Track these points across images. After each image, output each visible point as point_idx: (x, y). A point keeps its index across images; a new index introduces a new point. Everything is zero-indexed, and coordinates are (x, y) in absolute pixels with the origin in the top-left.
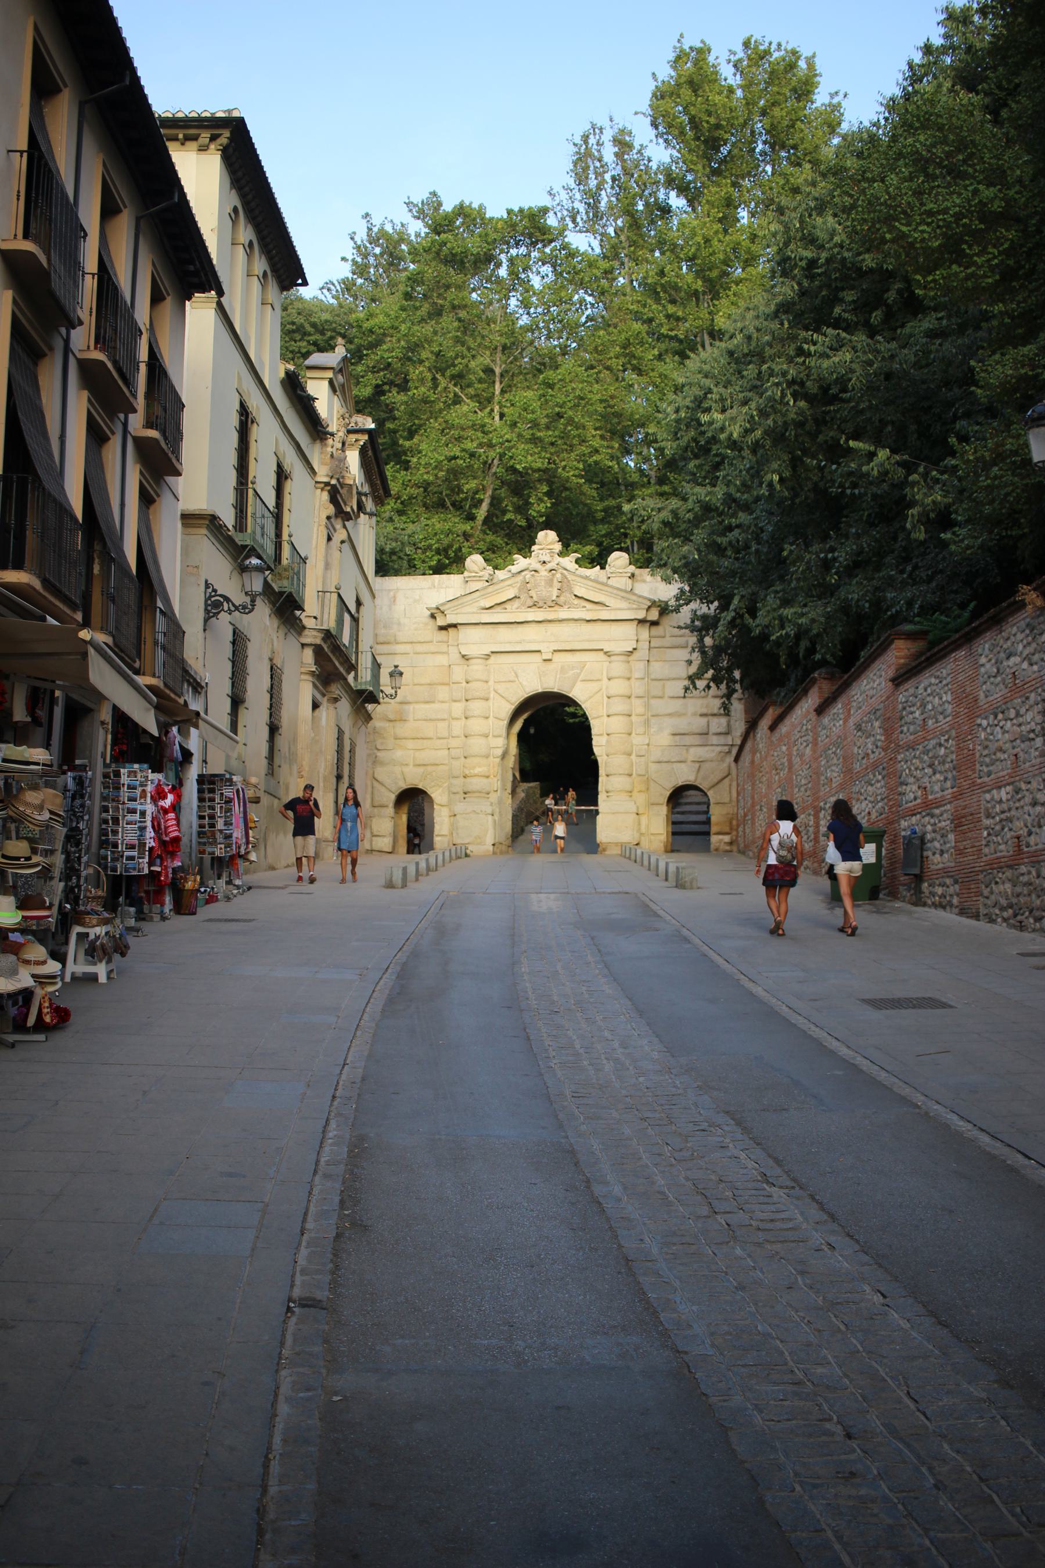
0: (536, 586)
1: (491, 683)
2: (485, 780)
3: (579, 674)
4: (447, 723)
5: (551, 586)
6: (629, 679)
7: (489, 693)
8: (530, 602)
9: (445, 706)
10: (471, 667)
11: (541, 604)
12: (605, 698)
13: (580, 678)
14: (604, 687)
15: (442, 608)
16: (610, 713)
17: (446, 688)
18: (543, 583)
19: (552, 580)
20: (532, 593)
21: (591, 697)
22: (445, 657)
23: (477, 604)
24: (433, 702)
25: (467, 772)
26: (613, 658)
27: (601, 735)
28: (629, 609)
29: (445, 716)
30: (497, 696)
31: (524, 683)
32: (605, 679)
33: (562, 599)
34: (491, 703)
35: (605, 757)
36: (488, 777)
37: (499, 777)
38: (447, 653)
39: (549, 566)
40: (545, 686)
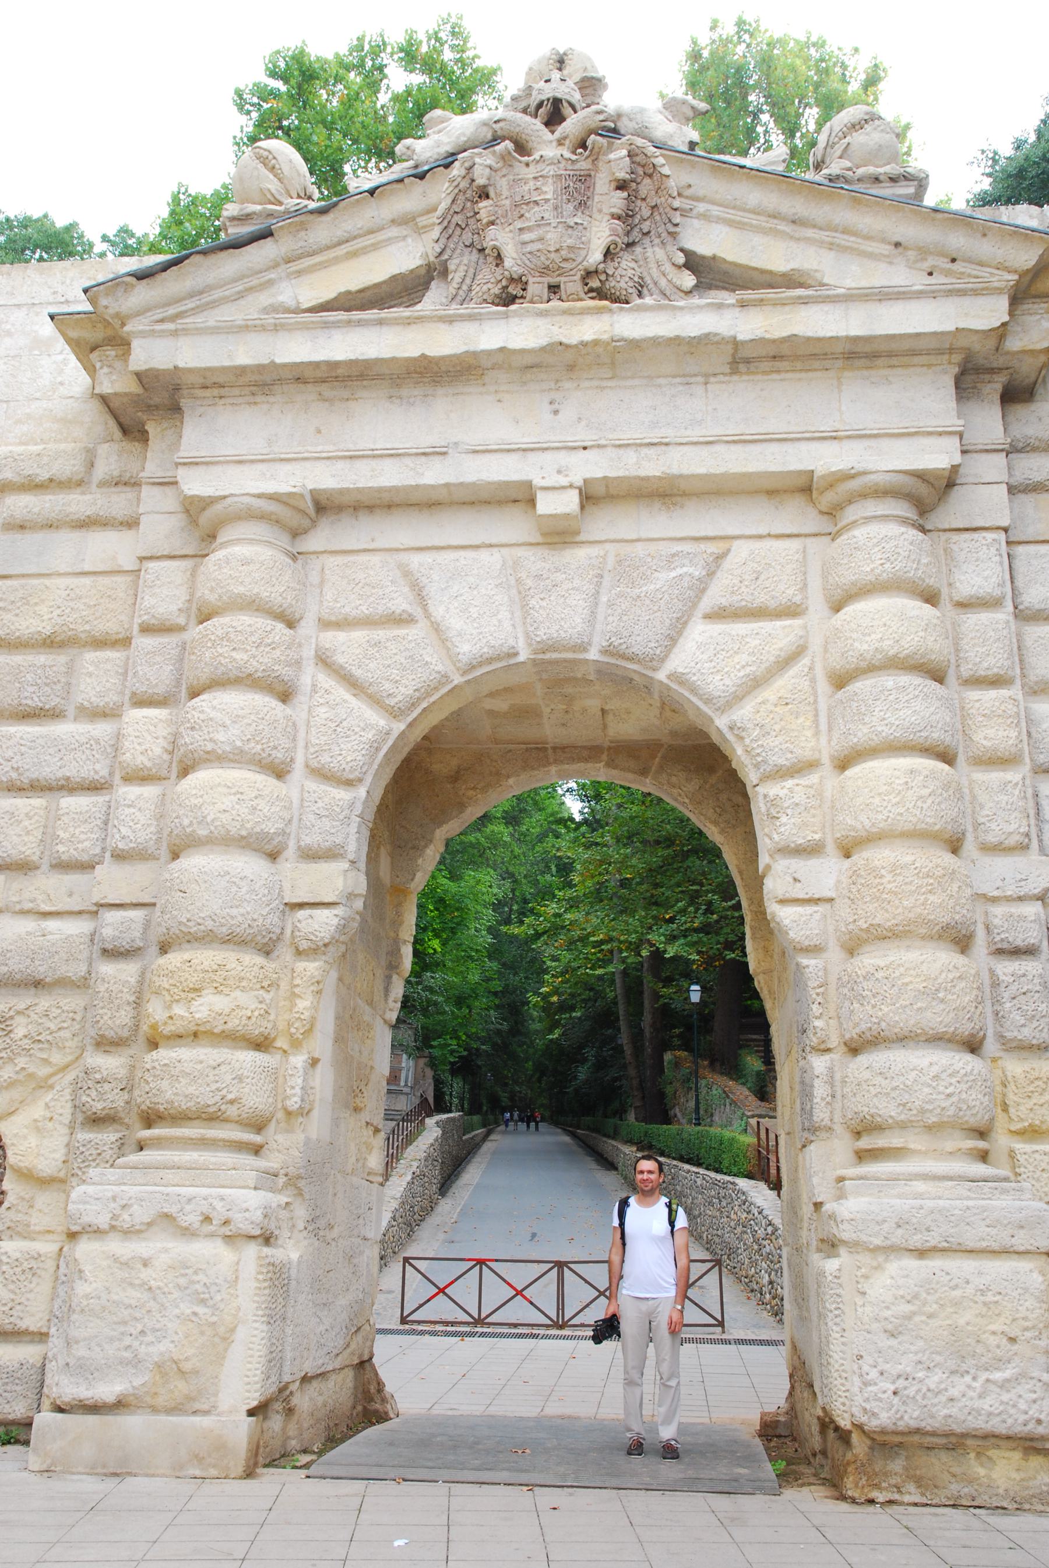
0: (522, 204)
1: (307, 628)
2: (247, 1057)
3: (701, 588)
4: (100, 799)
5: (582, 205)
6: (931, 598)
7: (298, 663)
8: (489, 281)
9: (102, 729)
10: (220, 554)
11: (536, 287)
12: (823, 686)
13: (707, 603)
14: (816, 644)
15: (111, 305)
16: (862, 734)
17: (113, 655)
18: (549, 190)
19: (585, 179)
20: (500, 237)
21: (755, 683)
22: (128, 535)
23: (264, 299)
24: (54, 714)
25: (156, 1011)
26: (852, 513)
27: (811, 850)
28: (932, 294)
29: (100, 770)
30: (325, 681)
31: (455, 623)
32: (817, 604)
33: (626, 268)
34: (299, 711)
35: (834, 954)
36: (261, 1044)
37: (322, 1044)
38: (131, 523)
39: (572, 125)
40: (546, 632)
